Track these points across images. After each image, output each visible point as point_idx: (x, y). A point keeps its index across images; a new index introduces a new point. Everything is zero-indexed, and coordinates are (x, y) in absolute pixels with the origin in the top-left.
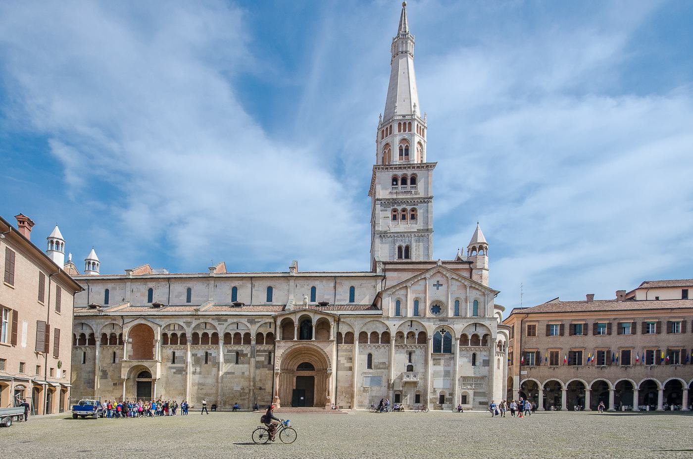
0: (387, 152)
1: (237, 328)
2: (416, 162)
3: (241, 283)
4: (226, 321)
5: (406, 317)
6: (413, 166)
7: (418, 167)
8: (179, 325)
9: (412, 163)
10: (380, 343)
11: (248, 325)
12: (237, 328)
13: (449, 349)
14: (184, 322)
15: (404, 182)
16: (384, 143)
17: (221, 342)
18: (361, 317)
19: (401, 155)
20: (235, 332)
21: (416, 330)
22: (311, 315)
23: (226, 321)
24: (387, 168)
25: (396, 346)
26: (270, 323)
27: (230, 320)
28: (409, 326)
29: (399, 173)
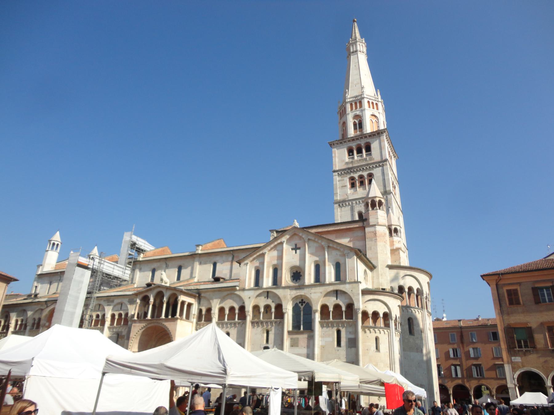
2: (368, 132)
3: (158, 264)
4: (113, 301)
5: (262, 288)
7: (370, 136)
9: (365, 133)
10: (236, 319)
13: (309, 327)
15: (359, 151)
16: (342, 123)
18: (219, 291)
19: (355, 128)
22: (164, 291)
24: (341, 143)
25: (253, 323)
27: (117, 301)
29: (354, 145)
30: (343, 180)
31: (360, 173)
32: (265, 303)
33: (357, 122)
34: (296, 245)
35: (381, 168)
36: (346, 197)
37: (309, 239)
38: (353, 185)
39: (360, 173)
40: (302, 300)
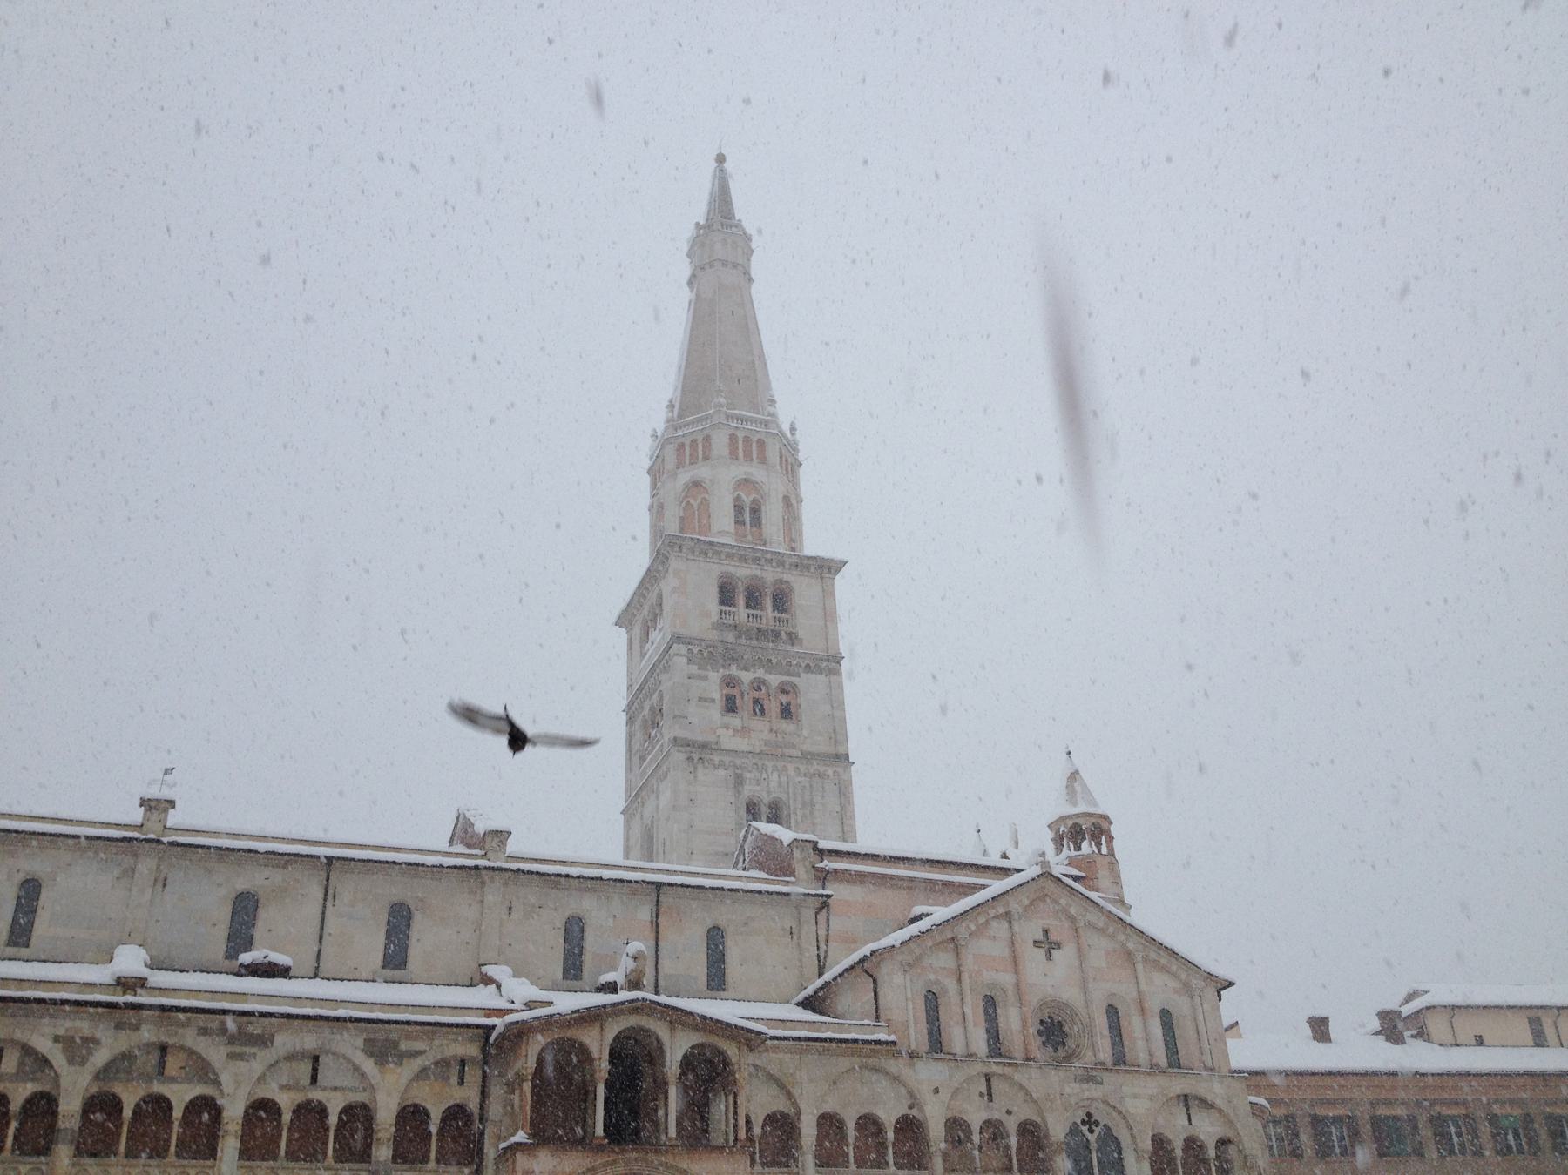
0: (695, 504)
1: (314, 1080)
3: (278, 876)
6: (779, 561)
8: (27, 1050)
11: (368, 1065)
12: (314, 1080)
14: (56, 1039)
16: (684, 477)
17: (229, 1146)
19: (739, 522)
20: (299, 1098)
21: (1009, 1113)
22: (661, 1030)
23: (263, 1041)
26: (463, 1063)
27: (284, 1041)
28: (981, 1095)
29: (742, 572)
30: (705, 678)
31: (760, 673)
32: (985, 1116)
33: (747, 500)
34: (1046, 931)
35: (821, 678)
36: (712, 738)
37: (1090, 925)
38: (731, 706)
39: (760, 673)
40: (1089, 1115)
